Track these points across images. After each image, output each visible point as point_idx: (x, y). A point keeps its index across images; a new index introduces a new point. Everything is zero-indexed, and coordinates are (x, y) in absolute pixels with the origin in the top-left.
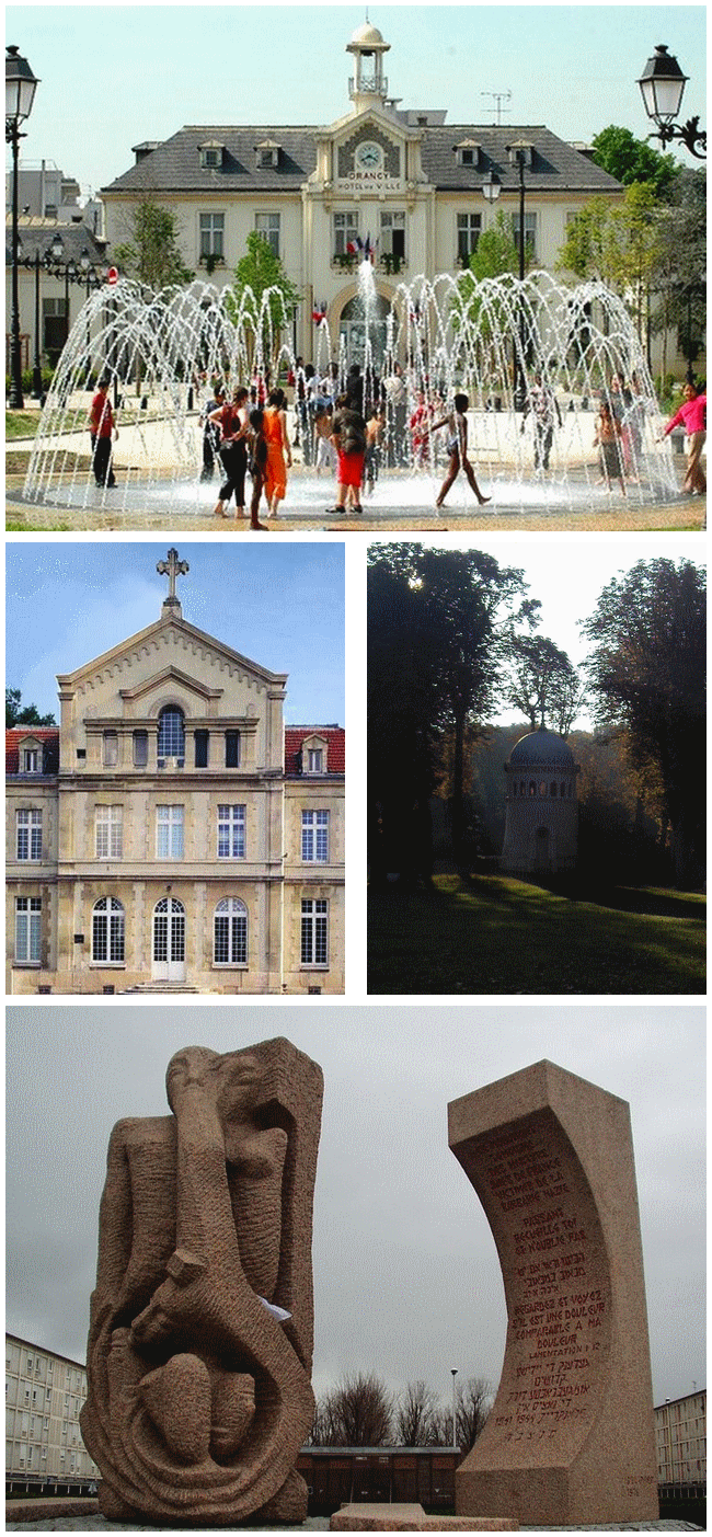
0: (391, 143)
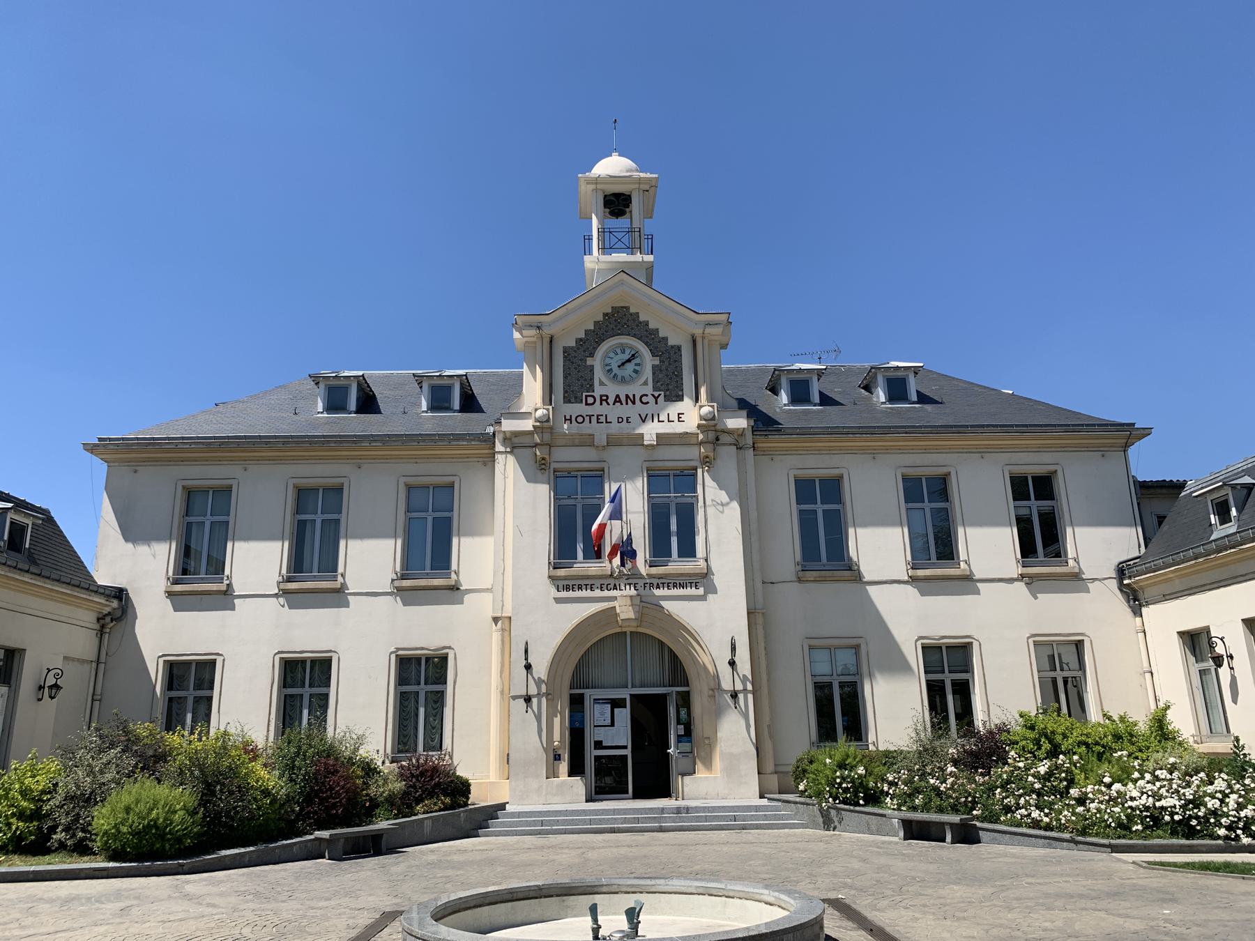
0: (665, 339)
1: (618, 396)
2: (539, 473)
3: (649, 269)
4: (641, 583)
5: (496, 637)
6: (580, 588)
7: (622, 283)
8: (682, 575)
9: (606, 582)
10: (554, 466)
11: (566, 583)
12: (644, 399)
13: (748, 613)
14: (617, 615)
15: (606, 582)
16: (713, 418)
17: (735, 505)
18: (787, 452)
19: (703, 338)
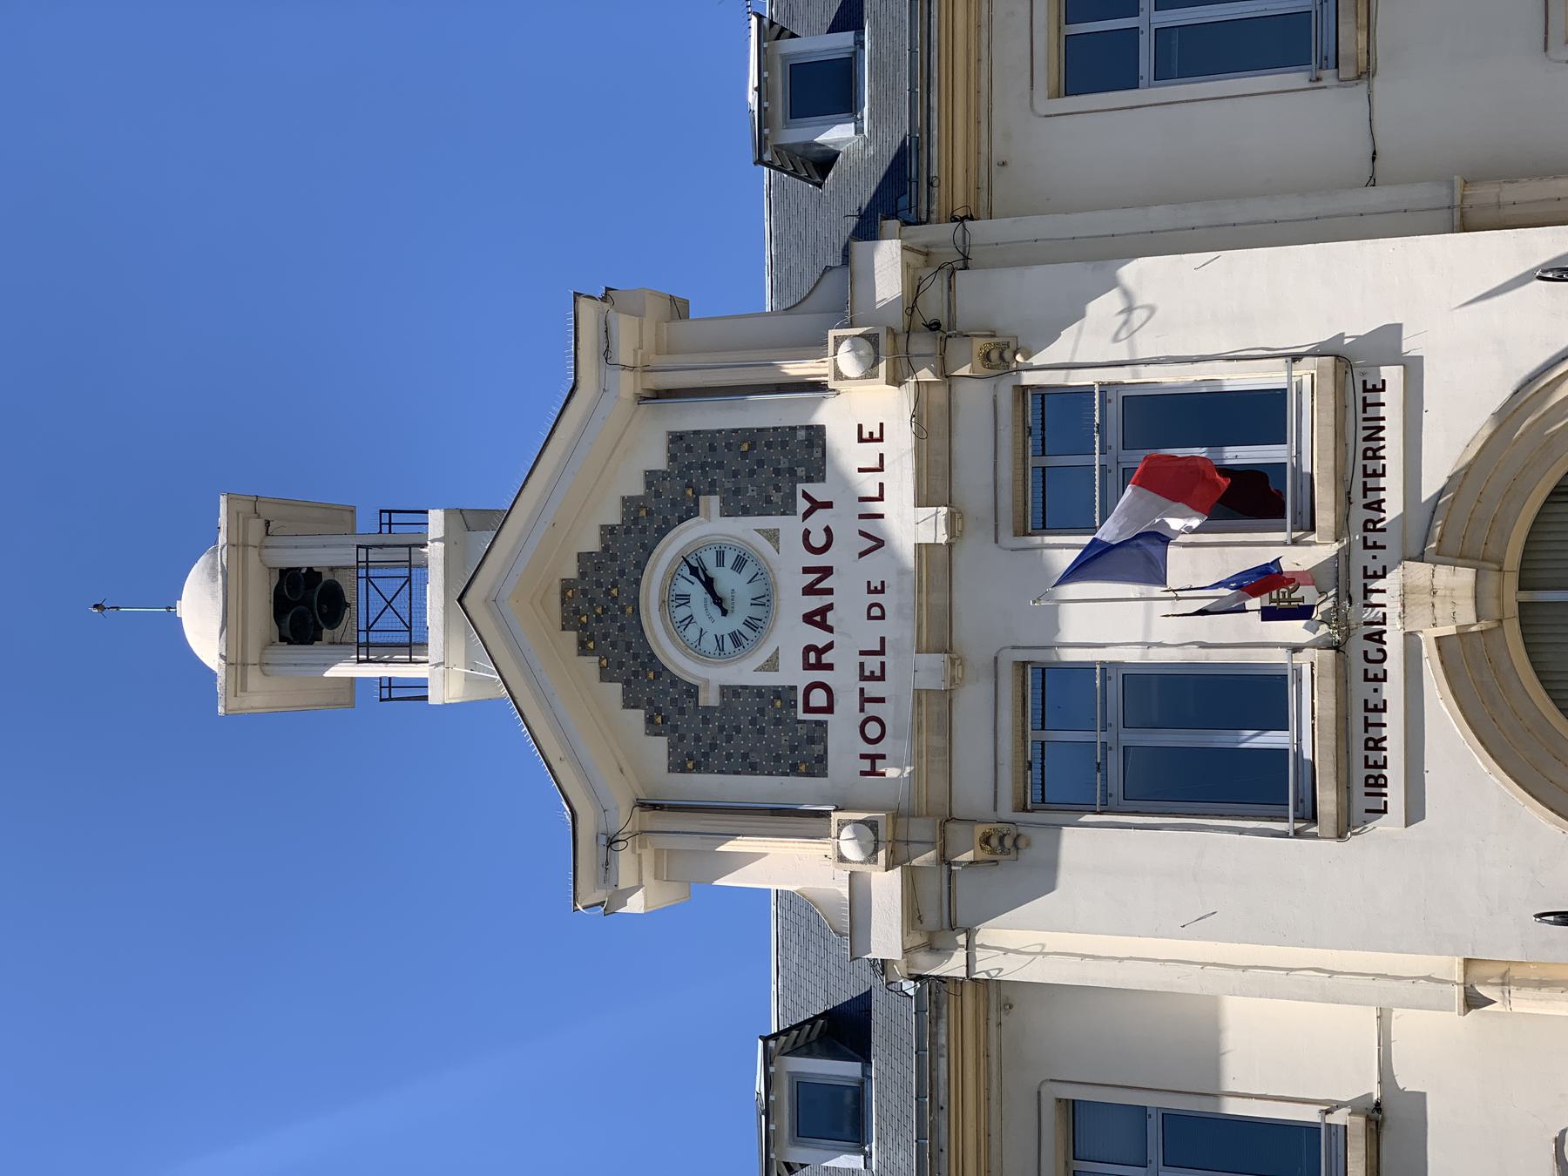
0: (651, 477)
1: (808, 618)
2: (1027, 855)
3: (466, 520)
4: (1361, 558)
5: (1525, 1003)
6: (1377, 744)
7: (493, 601)
8: (1339, 433)
9: (1358, 666)
10: (1006, 811)
11: (1359, 788)
12: (818, 540)
13: (1465, 228)
14: (1463, 634)
15: (1358, 666)
16: (872, 339)
17: (1133, 272)
18: (982, 117)
19: (647, 369)
